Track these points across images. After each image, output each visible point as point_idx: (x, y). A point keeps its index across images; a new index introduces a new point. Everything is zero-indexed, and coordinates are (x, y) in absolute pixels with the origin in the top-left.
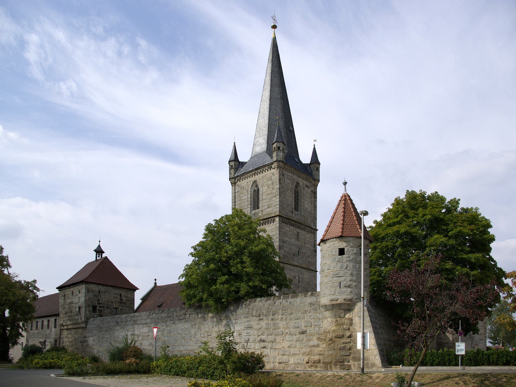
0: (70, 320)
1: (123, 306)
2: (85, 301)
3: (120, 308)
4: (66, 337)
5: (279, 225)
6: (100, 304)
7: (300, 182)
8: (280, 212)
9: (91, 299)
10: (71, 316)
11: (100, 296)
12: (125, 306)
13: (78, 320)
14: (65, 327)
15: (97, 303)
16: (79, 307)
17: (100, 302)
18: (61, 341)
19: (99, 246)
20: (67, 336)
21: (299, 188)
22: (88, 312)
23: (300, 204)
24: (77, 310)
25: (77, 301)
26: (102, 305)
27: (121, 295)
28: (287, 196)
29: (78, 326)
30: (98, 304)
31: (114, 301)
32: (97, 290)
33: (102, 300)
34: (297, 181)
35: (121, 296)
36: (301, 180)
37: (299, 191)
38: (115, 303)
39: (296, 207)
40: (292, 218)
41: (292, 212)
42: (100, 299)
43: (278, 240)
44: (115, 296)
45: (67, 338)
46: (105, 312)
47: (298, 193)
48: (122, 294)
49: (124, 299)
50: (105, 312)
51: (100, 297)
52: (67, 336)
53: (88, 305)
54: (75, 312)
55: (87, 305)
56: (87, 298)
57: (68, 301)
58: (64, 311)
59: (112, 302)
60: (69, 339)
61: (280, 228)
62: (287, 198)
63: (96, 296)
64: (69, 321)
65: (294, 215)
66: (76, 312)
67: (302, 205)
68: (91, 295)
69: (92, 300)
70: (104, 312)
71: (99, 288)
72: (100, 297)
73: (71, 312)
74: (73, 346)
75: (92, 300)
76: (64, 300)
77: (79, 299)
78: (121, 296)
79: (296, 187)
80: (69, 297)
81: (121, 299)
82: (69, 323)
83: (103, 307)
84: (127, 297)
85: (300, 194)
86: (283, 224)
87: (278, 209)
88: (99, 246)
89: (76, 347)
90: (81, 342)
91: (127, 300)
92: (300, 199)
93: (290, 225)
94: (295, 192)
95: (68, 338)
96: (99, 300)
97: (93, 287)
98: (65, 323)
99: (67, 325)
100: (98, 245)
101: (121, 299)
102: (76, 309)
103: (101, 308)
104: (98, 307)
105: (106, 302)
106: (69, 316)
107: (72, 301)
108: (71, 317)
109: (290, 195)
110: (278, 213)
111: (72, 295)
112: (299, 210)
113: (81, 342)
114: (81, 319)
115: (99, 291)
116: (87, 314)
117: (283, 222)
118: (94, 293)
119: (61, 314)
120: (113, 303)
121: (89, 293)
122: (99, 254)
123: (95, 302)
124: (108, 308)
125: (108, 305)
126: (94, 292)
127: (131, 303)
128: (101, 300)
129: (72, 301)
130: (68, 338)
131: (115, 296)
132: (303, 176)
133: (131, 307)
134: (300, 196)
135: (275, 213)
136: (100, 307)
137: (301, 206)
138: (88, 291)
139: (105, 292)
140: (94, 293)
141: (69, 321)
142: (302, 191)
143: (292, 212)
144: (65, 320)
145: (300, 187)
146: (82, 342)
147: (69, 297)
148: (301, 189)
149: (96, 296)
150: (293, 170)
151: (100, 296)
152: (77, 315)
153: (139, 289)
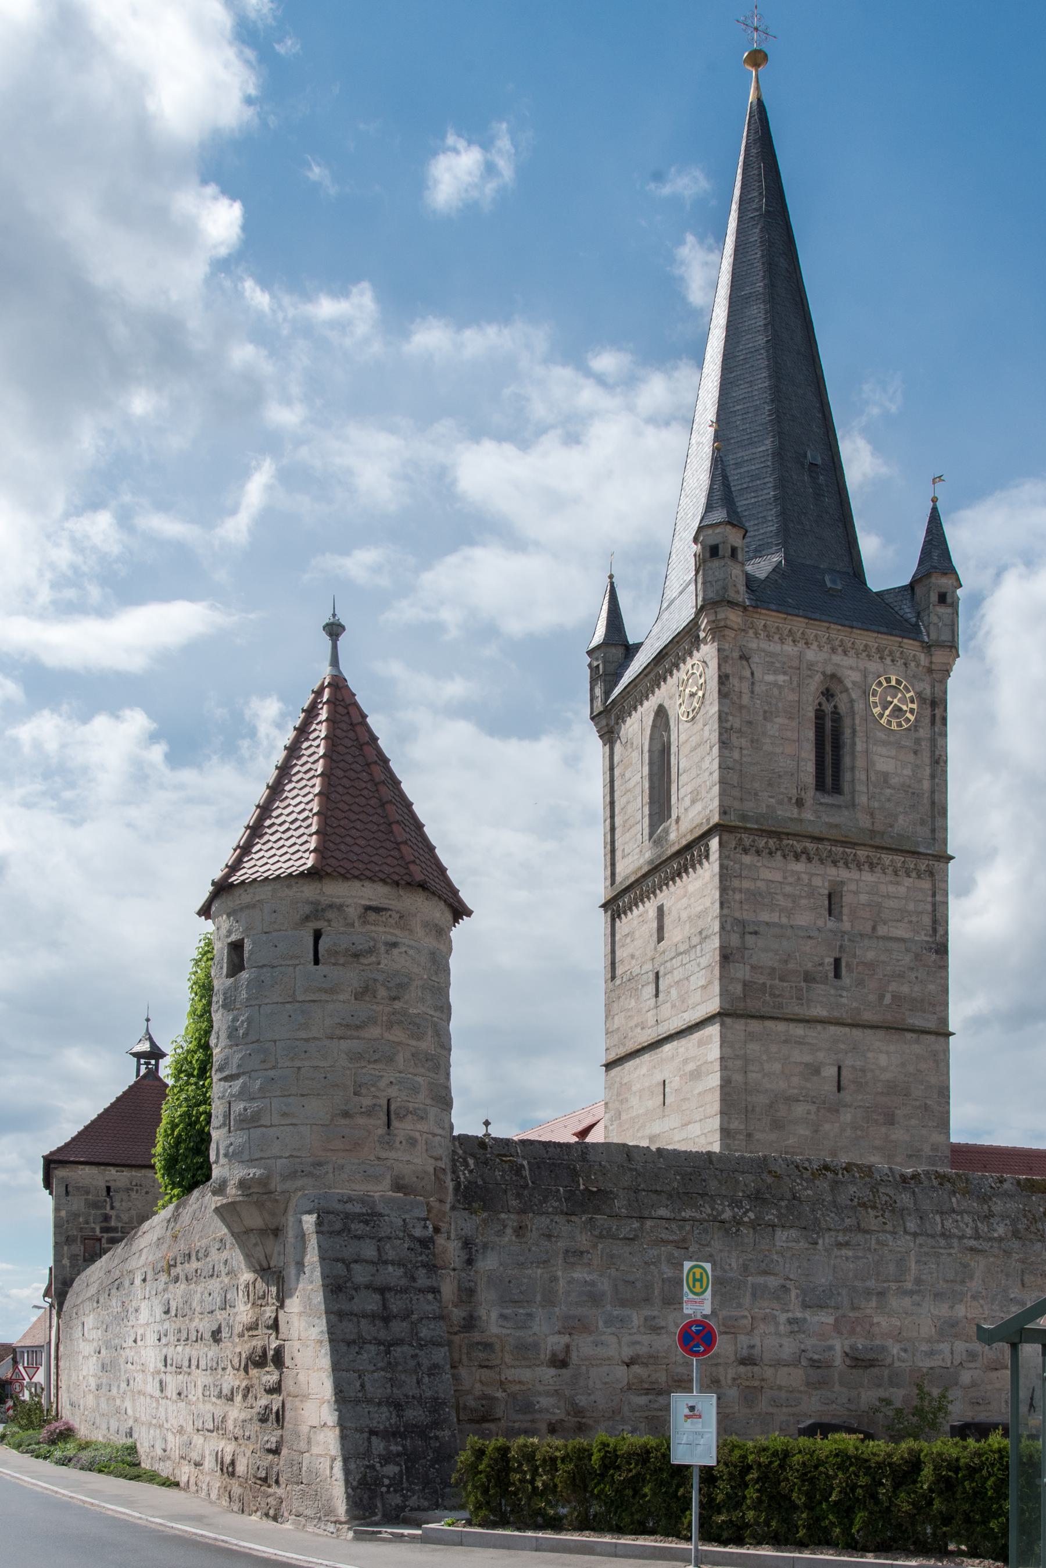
5: (722, 866)
7: (849, 672)
8: (723, 812)
9: (77, 1215)
11: (112, 1203)
15: (101, 1228)
17: (113, 1223)
21: (844, 696)
22: (66, 1262)
23: (847, 761)
28: (768, 741)
30: (106, 1230)
33: (118, 1217)
34: (829, 670)
36: (850, 661)
37: (843, 709)
39: (829, 781)
40: (793, 828)
41: (800, 803)
42: (113, 1213)
43: (716, 927)
47: (837, 717)
51: (112, 1208)
55: (63, 1239)
61: (725, 876)
62: (767, 748)
63: (96, 1205)
65: (808, 815)
67: (860, 763)
69: (81, 1220)
72: (112, 1208)
75: (81, 1220)
79: (828, 694)
85: (847, 722)
86: (747, 859)
87: (716, 803)
92: (848, 741)
93: (784, 856)
94: (820, 715)
96: (106, 1218)
104: (104, 1241)
109: (789, 734)
110: (716, 819)
112: (846, 787)
115: (108, 1189)
116: (64, 1267)
117: (746, 851)
118: (90, 1197)
123: (93, 1225)
126: (88, 1193)
132: (860, 644)
134: (847, 732)
135: (708, 820)
137: (853, 769)
139: (128, 1190)
140: (90, 1197)
142: (859, 706)
143: (800, 803)
145: (846, 690)
148: (852, 701)
150: (798, 624)
151: (112, 1203)
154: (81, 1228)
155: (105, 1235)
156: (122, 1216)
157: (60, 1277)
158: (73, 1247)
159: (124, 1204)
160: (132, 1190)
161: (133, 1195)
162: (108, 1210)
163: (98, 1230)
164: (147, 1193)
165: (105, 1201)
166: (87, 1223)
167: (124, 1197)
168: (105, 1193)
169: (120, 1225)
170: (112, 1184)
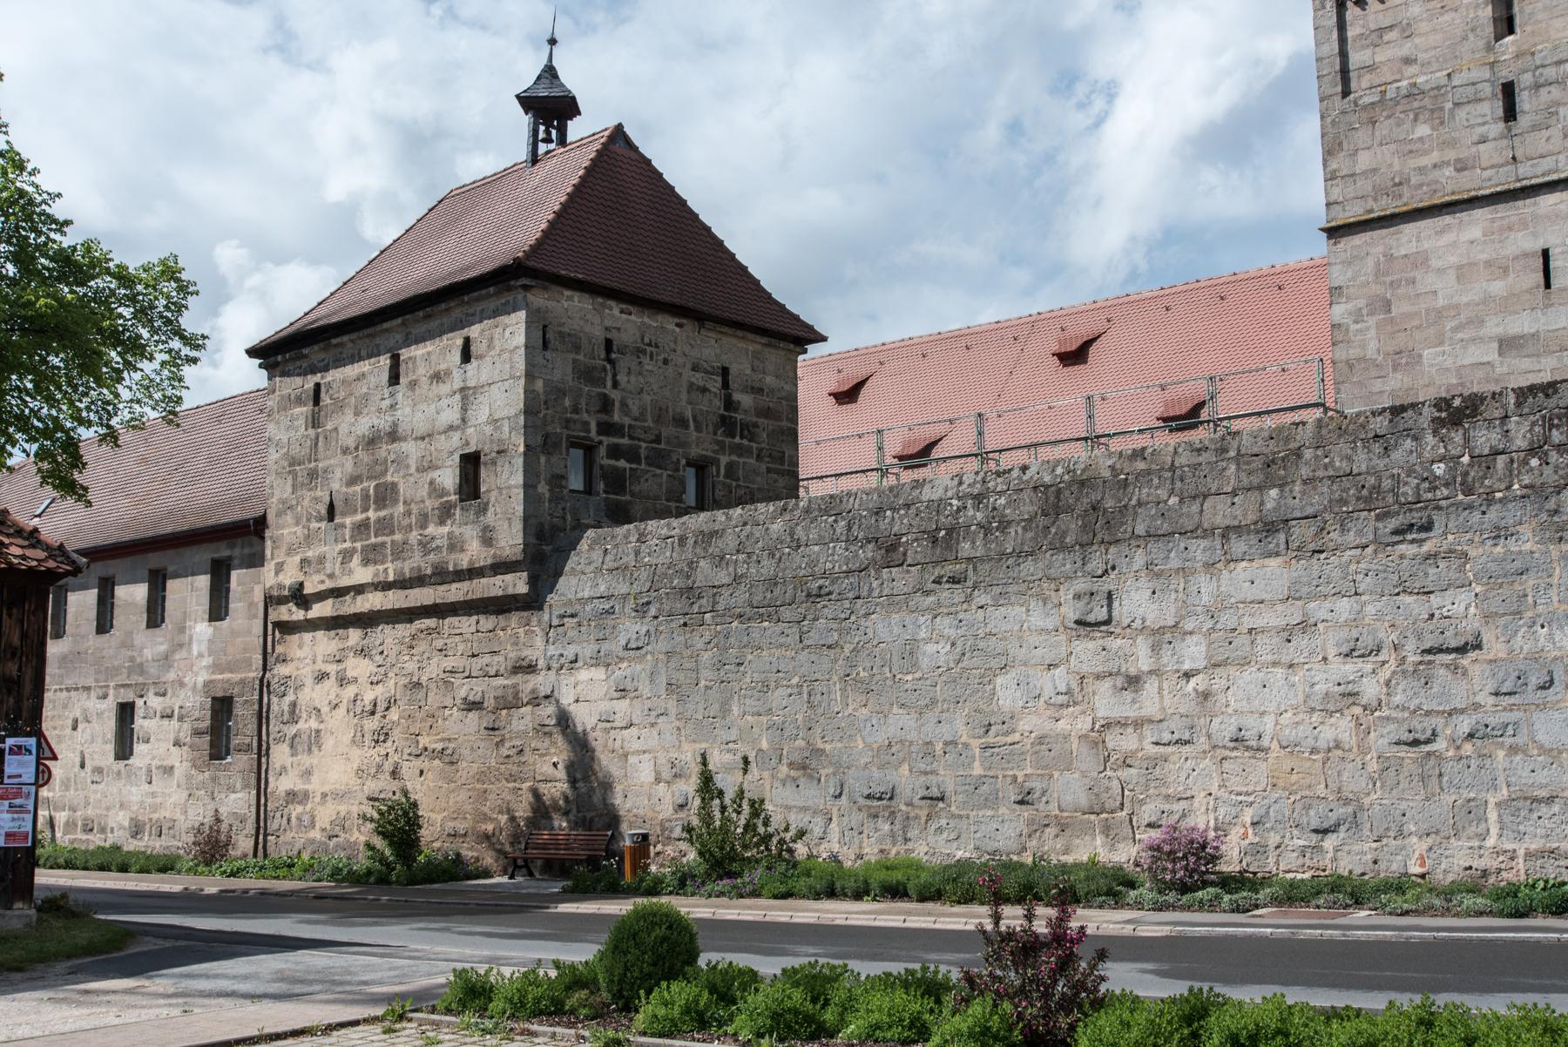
0: (371, 555)
1: (739, 450)
2: (529, 411)
4: (322, 677)
10: (385, 526)
11: (615, 375)
13: (455, 545)
14: (320, 610)
15: (599, 424)
16: (471, 464)
17: (617, 417)
18: (278, 706)
19: (550, 72)
20: (332, 668)
22: (543, 488)
24: (449, 477)
25: (451, 415)
26: (625, 441)
27: (725, 372)
29: (455, 592)
30: (607, 428)
31: (689, 414)
32: (598, 333)
33: (624, 404)
35: (726, 385)
42: (615, 395)
44: (698, 378)
45: (330, 684)
49: (745, 399)
51: (615, 385)
52: (332, 668)
53: (546, 436)
54: (424, 492)
55: (539, 440)
57: (350, 426)
58: (308, 495)
59: (681, 422)
60: (350, 691)
64: (356, 559)
66: (436, 490)
68: (561, 368)
71: (607, 323)
72: (615, 385)
73: (385, 495)
74: (396, 734)
75: (567, 402)
76: (315, 422)
77: (464, 399)
78: (726, 385)
80: (366, 397)
81: (729, 404)
82: (362, 575)
84: (760, 391)
88: (550, 72)
89: (424, 741)
90: (472, 706)
95: (342, 681)
96: (606, 405)
97: (573, 308)
98: (316, 578)
99: (338, 593)
100: (545, 61)
102: (435, 474)
103: (622, 463)
104: (602, 451)
105: (650, 423)
106: (362, 528)
107: (395, 425)
108: (385, 526)
111: (394, 379)
113: (472, 706)
114: (487, 539)
115: (609, 344)
116: (540, 499)
118: (581, 357)
119: (289, 518)
120: (687, 427)
122: (548, 126)
125: (658, 440)
128: (617, 404)
129: (395, 425)
130: (342, 681)
131: (698, 378)
133: (782, 460)
136: (615, 452)
138: (543, 339)
139: (639, 352)
141: (356, 559)
144: (321, 560)
146: (490, 703)
147: (366, 397)
149: (587, 374)
151: (615, 375)
152: (445, 513)
153: (824, 339)
154: (568, 421)
155: (606, 440)
156: (630, 402)
157: (532, 521)
158: (554, 459)
159: (633, 379)
162: (608, 389)
164: (666, 362)
165: (604, 369)
166: (576, 410)
168: (603, 355)
169: (627, 421)
170: (613, 335)
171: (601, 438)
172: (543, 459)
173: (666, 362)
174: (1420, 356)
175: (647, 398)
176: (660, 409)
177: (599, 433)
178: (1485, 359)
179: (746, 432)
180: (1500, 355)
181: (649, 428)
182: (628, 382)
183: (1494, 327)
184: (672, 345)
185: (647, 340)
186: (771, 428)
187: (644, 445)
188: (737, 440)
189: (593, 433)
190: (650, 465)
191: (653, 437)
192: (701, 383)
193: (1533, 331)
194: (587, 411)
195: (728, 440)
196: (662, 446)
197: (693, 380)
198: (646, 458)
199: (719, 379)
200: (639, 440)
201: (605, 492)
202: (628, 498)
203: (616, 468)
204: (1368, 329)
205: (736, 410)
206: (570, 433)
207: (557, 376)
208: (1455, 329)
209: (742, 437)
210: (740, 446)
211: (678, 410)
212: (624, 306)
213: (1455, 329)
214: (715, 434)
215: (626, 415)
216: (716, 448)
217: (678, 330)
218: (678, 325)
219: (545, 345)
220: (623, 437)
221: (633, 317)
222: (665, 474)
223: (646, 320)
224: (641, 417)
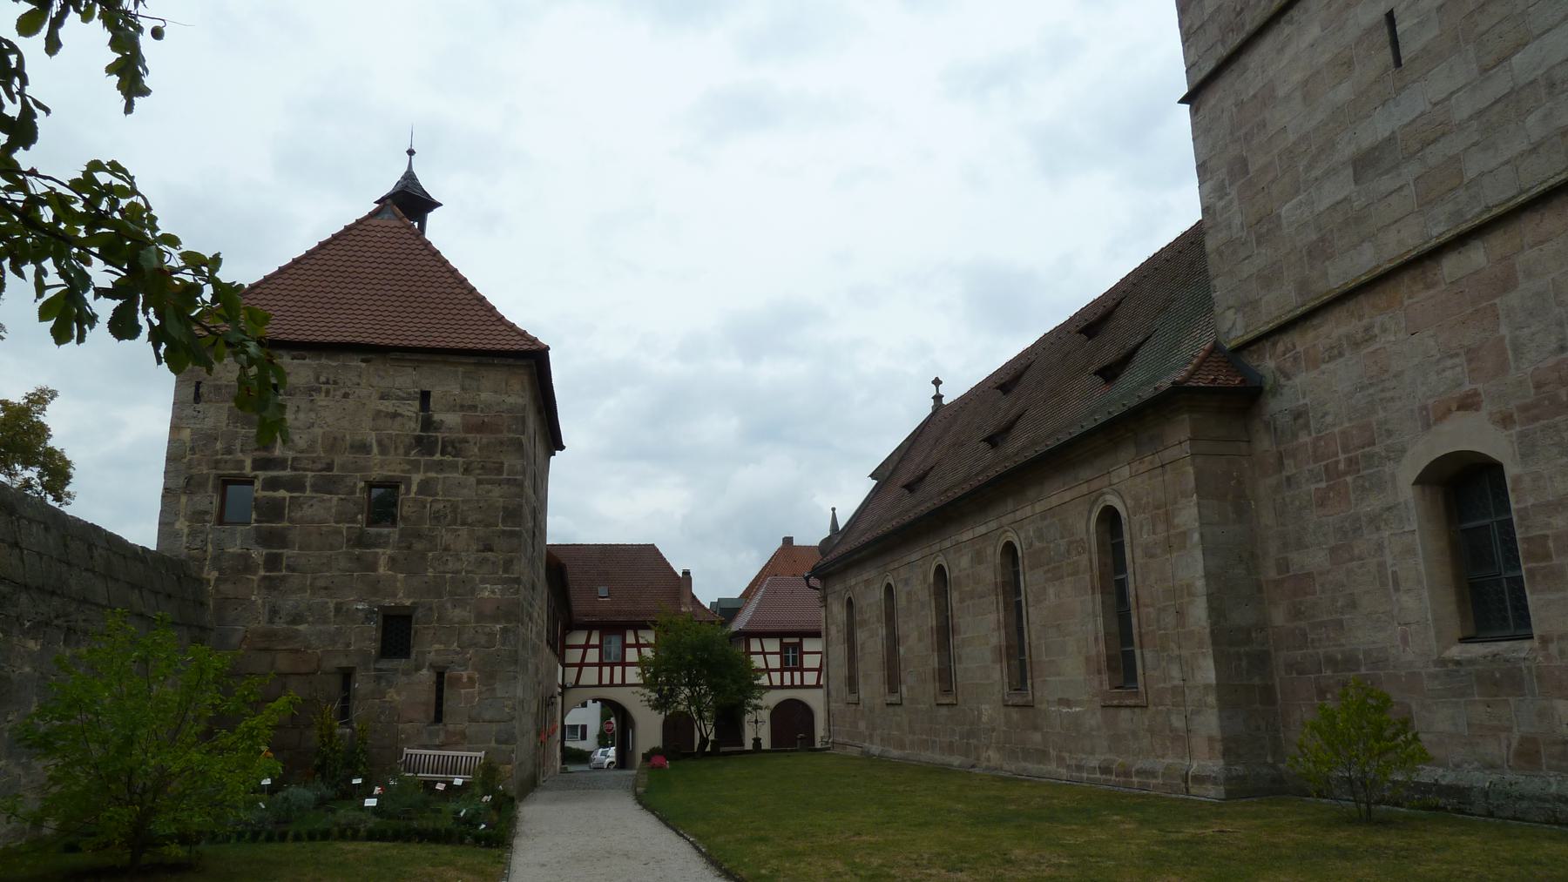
1: (440, 468)
3: (416, 478)
6: (280, 463)
9: (211, 438)
12: (454, 467)
15: (255, 461)
22: (182, 525)
26: (288, 473)
27: (425, 396)
31: (372, 438)
38: (383, 450)
44: (388, 406)
46: (308, 512)
48: (436, 394)
49: (451, 419)
50: (308, 512)
53: (189, 479)
55: (182, 482)
56: (186, 434)
59: (364, 448)
69: (219, 446)
70: (297, 515)
75: (219, 446)
81: (427, 424)
83: (296, 485)
91: (469, 428)
101: (427, 424)
103: (282, 493)
120: (369, 452)
121: (200, 407)
123: (240, 456)
124: (327, 485)
125: (329, 467)
127: (502, 443)
131: (388, 406)
136: (272, 484)
154: (217, 462)
155: (262, 474)
158: (197, 498)
159: (302, 416)
160: (319, 390)
161: (321, 400)
163: (248, 463)
166: (229, 451)
167: (303, 406)
169: (290, 454)
171: (257, 473)
172: (184, 499)
173: (346, 396)
174: (1279, 216)
175: (318, 431)
176: (335, 439)
177: (254, 469)
178: (1340, 197)
179: (450, 449)
180: (1356, 182)
181: (319, 458)
182: (296, 419)
183: (1346, 150)
184: (356, 380)
185: (322, 379)
186: (484, 441)
187: (310, 474)
188: (437, 457)
189: (248, 470)
190: (316, 491)
191: (324, 466)
192: (391, 410)
193: (1387, 134)
194: (242, 451)
195: (423, 459)
196: (335, 472)
197: (381, 408)
198: (312, 486)
199: (417, 404)
200: (305, 470)
201: (256, 521)
202: (286, 524)
203: (275, 499)
204: (1231, 202)
205: (437, 429)
206: (220, 472)
207: (209, 423)
208: (1309, 167)
209: (443, 453)
210: (441, 463)
211: (358, 438)
212: (295, 353)
213: (1309, 167)
214: (407, 453)
215: (290, 449)
216: (408, 467)
217: (364, 365)
218: (363, 361)
219: (197, 398)
220: (284, 469)
221: (307, 361)
222: (335, 498)
223: (324, 361)
224: (311, 446)
